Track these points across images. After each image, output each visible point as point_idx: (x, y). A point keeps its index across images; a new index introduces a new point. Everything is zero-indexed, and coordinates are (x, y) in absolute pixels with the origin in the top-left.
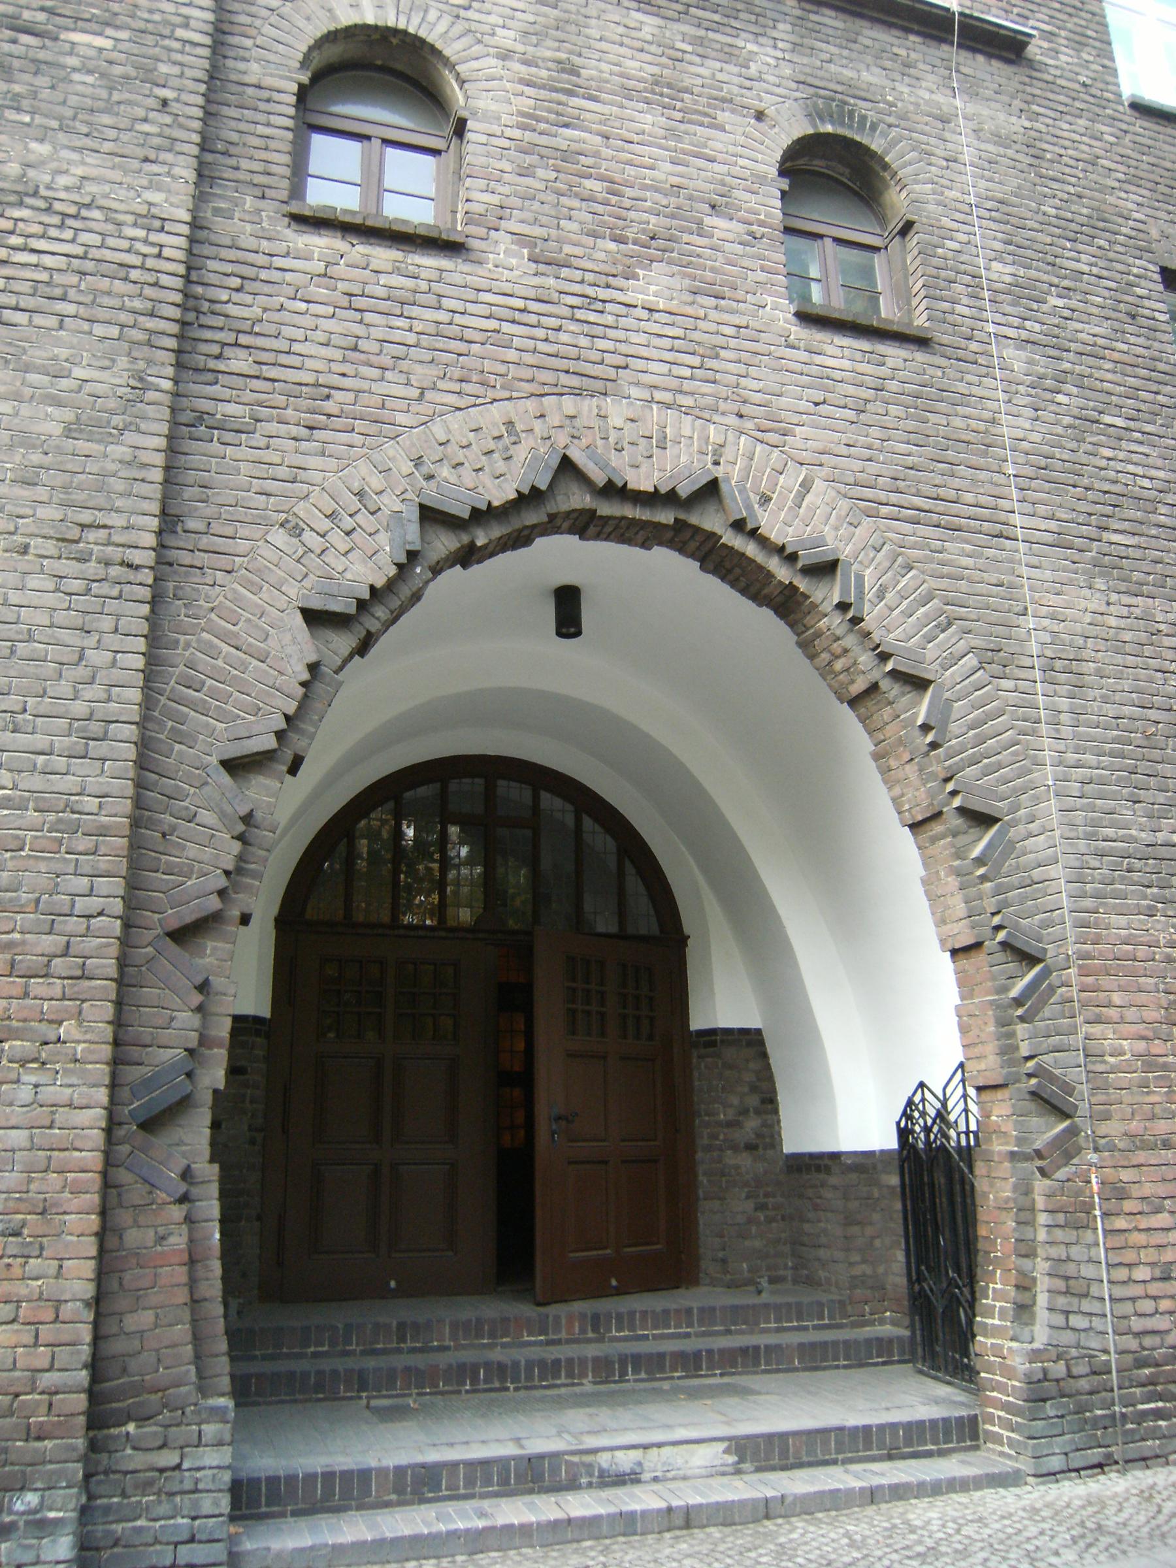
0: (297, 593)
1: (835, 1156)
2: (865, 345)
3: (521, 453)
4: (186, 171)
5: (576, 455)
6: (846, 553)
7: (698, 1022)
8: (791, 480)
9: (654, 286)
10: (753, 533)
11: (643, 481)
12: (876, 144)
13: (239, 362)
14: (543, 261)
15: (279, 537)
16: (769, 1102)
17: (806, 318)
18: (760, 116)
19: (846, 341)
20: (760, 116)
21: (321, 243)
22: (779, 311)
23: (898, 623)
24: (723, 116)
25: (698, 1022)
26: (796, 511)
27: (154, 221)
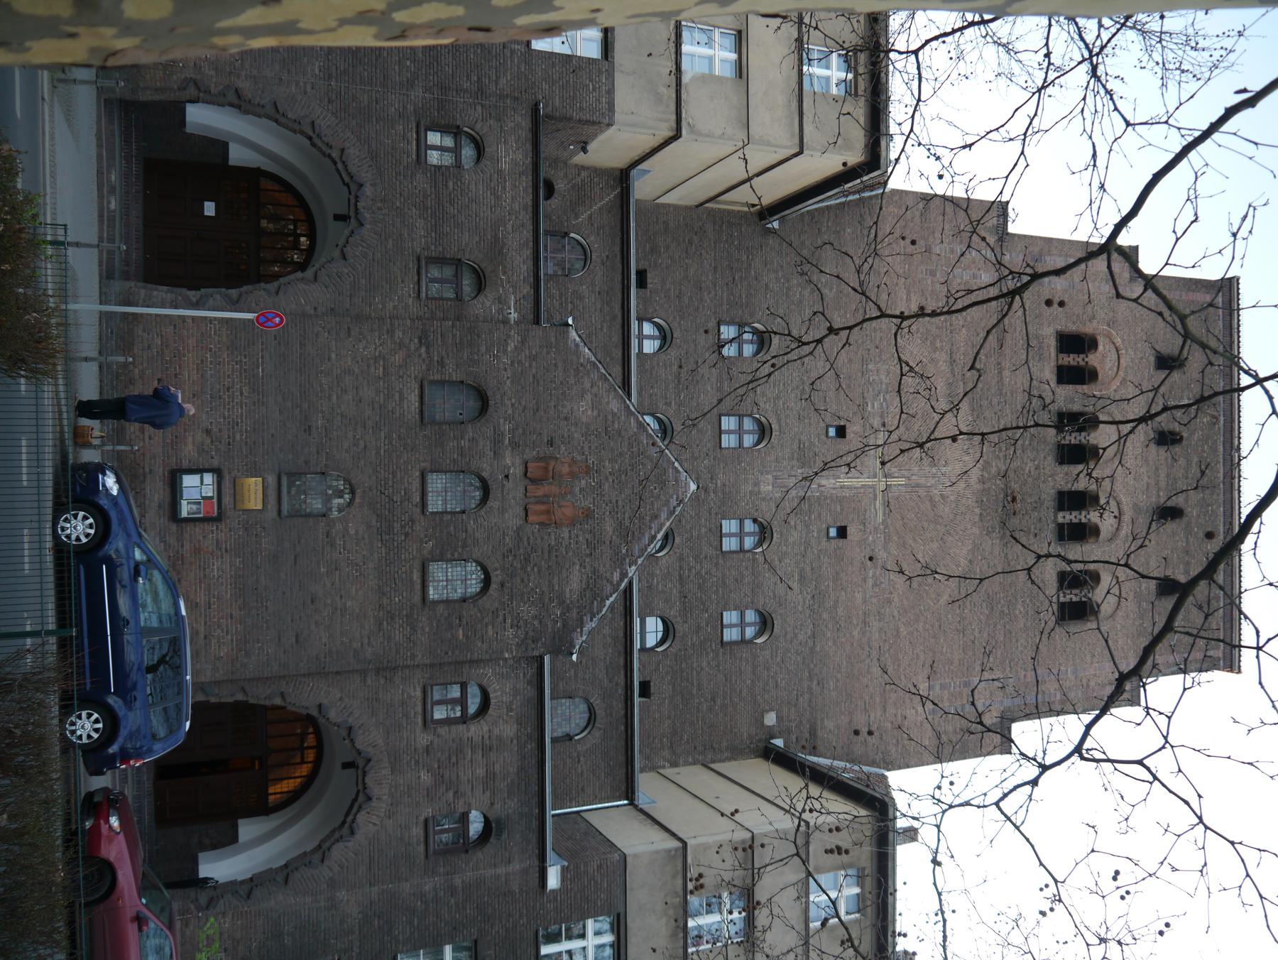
0: (325, 702)
1: (197, 865)
2: (422, 839)
3: (370, 749)
4: (428, 661)
5: (371, 763)
6: (357, 836)
7: (240, 821)
8: (374, 819)
9: (425, 777)
10: (358, 811)
11: (367, 780)
13: (382, 681)
14: (428, 749)
15: (338, 696)
16: (215, 847)
17: (426, 821)
18: (492, 804)
19: (422, 833)
20: (492, 804)
21: (419, 693)
22: (428, 812)
23: (338, 853)
24: (488, 793)
25: (240, 821)
26: (367, 822)
27: (413, 656)
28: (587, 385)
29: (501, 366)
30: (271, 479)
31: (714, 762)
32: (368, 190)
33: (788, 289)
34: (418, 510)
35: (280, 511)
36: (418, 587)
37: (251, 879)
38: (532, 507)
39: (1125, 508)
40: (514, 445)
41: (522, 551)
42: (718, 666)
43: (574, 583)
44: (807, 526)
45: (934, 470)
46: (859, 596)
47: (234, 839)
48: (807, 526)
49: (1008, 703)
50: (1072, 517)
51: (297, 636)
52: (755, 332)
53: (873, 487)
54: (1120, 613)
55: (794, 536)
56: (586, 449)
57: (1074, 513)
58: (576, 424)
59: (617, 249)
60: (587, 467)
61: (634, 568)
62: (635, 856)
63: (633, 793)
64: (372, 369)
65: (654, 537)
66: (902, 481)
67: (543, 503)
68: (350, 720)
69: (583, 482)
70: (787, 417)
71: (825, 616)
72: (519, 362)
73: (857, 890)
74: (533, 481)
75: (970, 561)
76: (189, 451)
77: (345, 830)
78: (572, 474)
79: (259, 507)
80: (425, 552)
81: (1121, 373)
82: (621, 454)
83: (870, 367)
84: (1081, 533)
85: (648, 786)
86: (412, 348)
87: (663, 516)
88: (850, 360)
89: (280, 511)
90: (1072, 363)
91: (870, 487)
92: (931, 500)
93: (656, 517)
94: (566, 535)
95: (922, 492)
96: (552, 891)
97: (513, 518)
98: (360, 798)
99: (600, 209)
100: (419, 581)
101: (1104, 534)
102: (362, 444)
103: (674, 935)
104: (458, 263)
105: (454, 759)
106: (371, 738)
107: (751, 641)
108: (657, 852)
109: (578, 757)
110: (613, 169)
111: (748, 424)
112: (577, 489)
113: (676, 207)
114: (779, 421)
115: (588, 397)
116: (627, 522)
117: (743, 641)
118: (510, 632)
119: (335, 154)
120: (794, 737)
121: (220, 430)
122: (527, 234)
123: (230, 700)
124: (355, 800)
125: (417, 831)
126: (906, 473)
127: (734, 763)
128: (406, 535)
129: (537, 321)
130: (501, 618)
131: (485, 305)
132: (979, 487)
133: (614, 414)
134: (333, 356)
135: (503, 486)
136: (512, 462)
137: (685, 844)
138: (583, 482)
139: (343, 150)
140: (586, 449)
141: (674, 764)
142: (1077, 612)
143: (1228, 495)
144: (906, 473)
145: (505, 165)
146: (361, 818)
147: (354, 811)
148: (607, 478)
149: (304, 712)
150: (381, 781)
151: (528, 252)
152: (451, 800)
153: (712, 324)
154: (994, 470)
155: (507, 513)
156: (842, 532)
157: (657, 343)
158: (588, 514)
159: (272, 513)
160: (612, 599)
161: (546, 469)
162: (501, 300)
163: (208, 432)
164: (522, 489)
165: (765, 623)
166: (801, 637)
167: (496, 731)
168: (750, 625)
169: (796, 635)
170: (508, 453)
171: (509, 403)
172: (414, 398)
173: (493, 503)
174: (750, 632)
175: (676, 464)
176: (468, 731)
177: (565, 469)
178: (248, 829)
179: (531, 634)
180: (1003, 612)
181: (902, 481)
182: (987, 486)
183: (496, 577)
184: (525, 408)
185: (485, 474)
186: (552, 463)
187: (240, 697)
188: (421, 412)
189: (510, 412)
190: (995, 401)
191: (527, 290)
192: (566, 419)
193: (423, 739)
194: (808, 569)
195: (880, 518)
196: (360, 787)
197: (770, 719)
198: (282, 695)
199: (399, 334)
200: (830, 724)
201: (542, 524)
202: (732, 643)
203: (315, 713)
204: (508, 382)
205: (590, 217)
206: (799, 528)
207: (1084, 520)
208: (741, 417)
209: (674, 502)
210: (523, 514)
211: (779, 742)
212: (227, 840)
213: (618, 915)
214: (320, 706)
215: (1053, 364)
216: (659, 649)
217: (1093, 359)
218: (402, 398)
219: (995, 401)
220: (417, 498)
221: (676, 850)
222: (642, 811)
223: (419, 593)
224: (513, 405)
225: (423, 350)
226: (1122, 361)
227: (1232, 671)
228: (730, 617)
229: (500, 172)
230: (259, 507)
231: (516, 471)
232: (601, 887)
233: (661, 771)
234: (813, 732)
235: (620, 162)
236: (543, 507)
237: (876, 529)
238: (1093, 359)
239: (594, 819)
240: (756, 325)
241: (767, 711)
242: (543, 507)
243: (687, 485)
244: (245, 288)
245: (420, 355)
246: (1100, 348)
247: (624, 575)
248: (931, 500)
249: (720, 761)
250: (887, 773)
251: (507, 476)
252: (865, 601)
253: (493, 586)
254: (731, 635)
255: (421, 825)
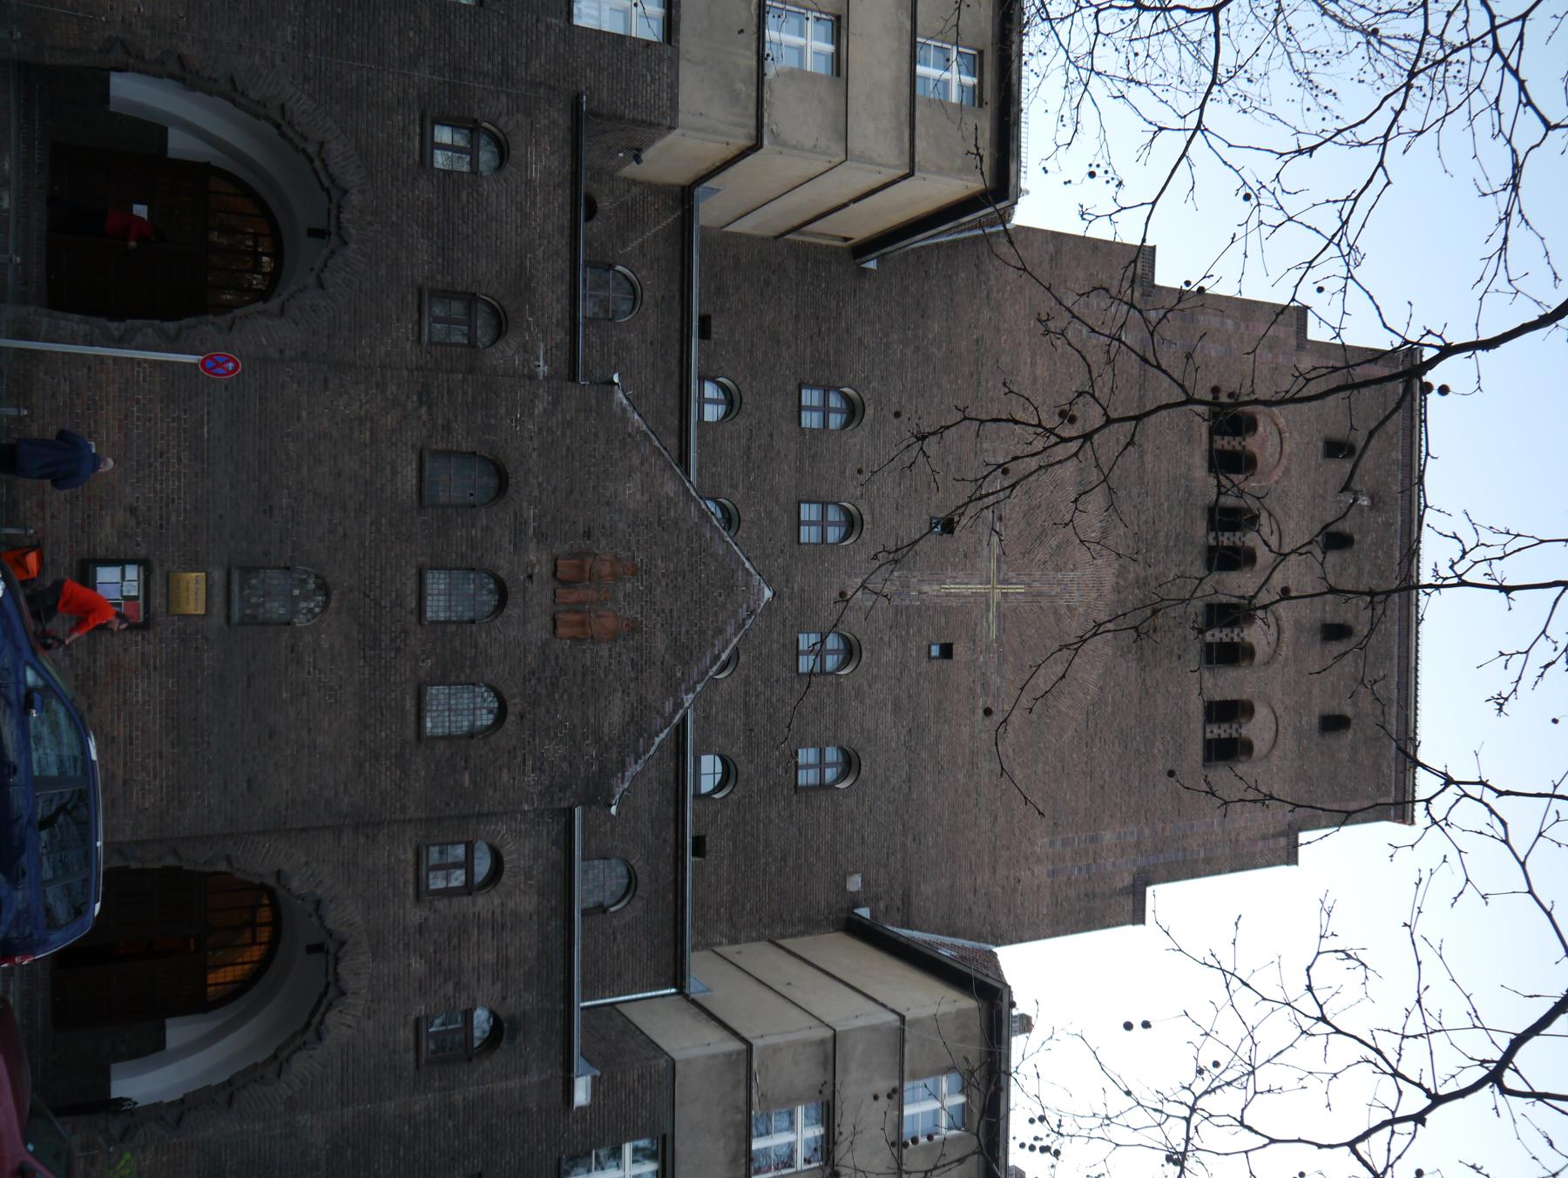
1: (108, 1080)
2: (412, 1045)
4: (423, 815)
5: (346, 947)
7: (168, 1022)
9: (417, 965)
10: (328, 1009)
11: (339, 969)
12: (503, 1044)
13: (362, 840)
15: (304, 860)
17: (417, 1021)
18: (504, 998)
19: (411, 1036)
20: (504, 998)
21: (410, 856)
22: (420, 1009)
23: (300, 1064)
24: (499, 985)
25: (168, 1022)
26: (340, 1024)
27: (404, 808)
28: (636, 461)
29: (526, 434)
30: (218, 575)
31: (783, 937)
32: (355, 198)
33: (887, 346)
34: (414, 619)
35: (228, 618)
36: (412, 718)
37: (182, 1100)
38: (561, 616)
39: (1285, 625)
40: (541, 537)
41: (548, 673)
42: (791, 817)
43: (614, 715)
44: (904, 643)
45: (1059, 576)
46: (965, 730)
47: (160, 1045)
48: (904, 643)
49: (1141, 862)
50: (1223, 635)
51: (249, 781)
52: (845, 397)
53: (985, 595)
54: (1276, 753)
55: (888, 656)
56: (633, 542)
57: (1226, 631)
58: (621, 511)
59: (675, 288)
60: (635, 566)
61: (691, 696)
62: (687, 1062)
63: (683, 978)
64: (357, 433)
65: (718, 657)
66: (1021, 589)
67: (577, 612)
68: (319, 892)
69: (629, 585)
70: (882, 506)
71: (924, 755)
72: (549, 430)
73: (961, 1099)
74: (565, 583)
75: (1101, 689)
76: (106, 535)
77: (310, 1034)
78: (615, 576)
79: (201, 611)
80: (422, 673)
81: (1284, 461)
82: (677, 552)
83: (985, 446)
84: (1232, 655)
85: (702, 969)
86: (410, 407)
87: (730, 630)
88: (961, 437)
89: (228, 618)
90: (1227, 447)
91: (982, 595)
92: (1056, 613)
93: (720, 631)
94: (606, 653)
95: (1045, 603)
96: (581, 1108)
97: (537, 630)
98: (331, 992)
99: (655, 236)
100: (413, 710)
101: (1260, 655)
102: (340, 530)
103: (734, 1160)
104: (470, 299)
105: (455, 941)
106: (346, 915)
107: (831, 786)
108: (714, 1056)
109: (614, 933)
110: (672, 185)
111: (833, 514)
112: (621, 595)
113: (749, 237)
114: (872, 511)
115: (637, 476)
116: (683, 638)
117: (822, 786)
118: (531, 778)
119: (311, 149)
120: (882, 905)
121: (149, 509)
122: (562, 264)
123: (157, 865)
124: (324, 994)
125: (405, 1035)
126: (1026, 578)
127: (807, 939)
128: (398, 650)
129: (573, 377)
130: (519, 759)
131: (505, 355)
132: (1113, 597)
133: (669, 500)
134: (304, 414)
135: (525, 589)
136: (537, 558)
137: (750, 1046)
138: (629, 585)
139: (322, 144)
140: (633, 542)
141: (734, 941)
142: (1225, 751)
143: (1404, 612)
144: (1026, 578)
145: (535, 174)
146: (332, 1018)
147: (322, 1009)
148: (659, 582)
149: (257, 881)
150: (358, 971)
151: (563, 288)
152: (451, 993)
153: (792, 387)
154: (1131, 576)
155: (529, 625)
156: (947, 651)
157: (722, 409)
158: (634, 627)
159: (218, 619)
160: (662, 736)
161: (581, 568)
162: (527, 349)
163: (133, 510)
164: (549, 594)
165: (850, 763)
166: (893, 781)
167: (511, 904)
168: (831, 765)
169: (887, 779)
170: (532, 546)
171: (533, 481)
172: (410, 472)
173: (512, 611)
174: (830, 774)
175: (747, 565)
176: (474, 904)
177: (606, 569)
178: (178, 1032)
179: (558, 779)
180: (1138, 750)
181: (1021, 589)
182: (1122, 596)
183: (515, 705)
184: (555, 489)
185: (501, 573)
186: (590, 560)
187: (170, 861)
188: (420, 490)
189: (535, 493)
190: (1135, 491)
191: (561, 336)
192: (608, 504)
193: (415, 915)
194: (904, 696)
195: (993, 635)
196: (331, 978)
197: (855, 883)
198: (228, 859)
199: (392, 389)
200: (927, 889)
201: (575, 639)
202: (808, 788)
203: (271, 882)
204: (535, 455)
205: (642, 246)
206: (894, 645)
207: (1236, 639)
208: (824, 505)
209: (743, 613)
210: (550, 626)
211: (864, 912)
212: (150, 1046)
213: (664, 1137)
214: (279, 873)
215: (1205, 446)
216: (717, 796)
217: (1251, 443)
218: (394, 472)
219: (1135, 491)
220: (412, 603)
221: (739, 1053)
222: (694, 1002)
223: (413, 726)
224: (540, 485)
225: (424, 410)
226: (1286, 446)
227: (1404, 822)
228: (807, 755)
229: (529, 182)
230: (201, 611)
231: (543, 570)
232: (643, 1102)
233: (718, 949)
234: (906, 899)
235: (679, 174)
236: (577, 617)
237: (988, 648)
238: (1251, 443)
239: (636, 1015)
240: (846, 390)
241: (851, 874)
242: (577, 617)
243: (760, 591)
244: (185, 322)
245: (419, 417)
246: (1260, 429)
247: (678, 705)
248: (1056, 613)
249: (791, 936)
250: (996, 950)
251: (530, 577)
252: (972, 737)
253: (510, 718)
254: (807, 777)
255: (411, 1028)
